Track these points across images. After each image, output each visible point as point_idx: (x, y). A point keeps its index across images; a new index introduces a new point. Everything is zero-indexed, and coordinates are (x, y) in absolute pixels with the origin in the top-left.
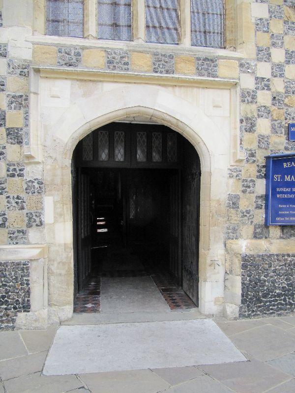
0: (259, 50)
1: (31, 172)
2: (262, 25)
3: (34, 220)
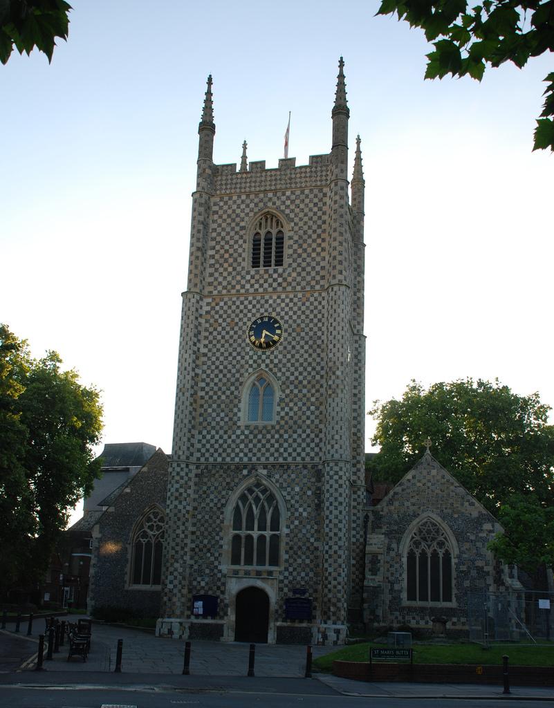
0: (285, 568)
1: (226, 601)
2: (287, 561)
3: (226, 614)
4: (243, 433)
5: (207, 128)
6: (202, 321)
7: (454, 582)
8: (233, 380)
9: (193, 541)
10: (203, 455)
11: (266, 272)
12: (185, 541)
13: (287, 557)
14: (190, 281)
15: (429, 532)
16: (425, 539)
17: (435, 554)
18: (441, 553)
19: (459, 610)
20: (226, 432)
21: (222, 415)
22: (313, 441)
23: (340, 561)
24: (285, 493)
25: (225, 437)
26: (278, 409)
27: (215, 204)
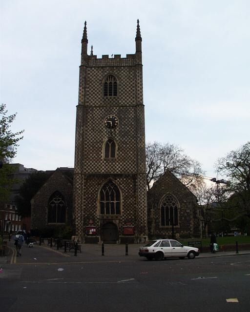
2: (123, 212)
4: (103, 162)
5: (85, 41)
7: (179, 218)
8: (98, 141)
9: (84, 206)
10: (87, 171)
11: (111, 98)
13: (123, 211)
14: (79, 101)
15: (169, 200)
17: (171, 208)
18: (174, 207)
20: (96, 162)
21: (94, 155)
22: (132, 165)
23: (145, 212)
24: (121, 186)
25: (96, 164)
26: (118, 153)
27: (89, 70)
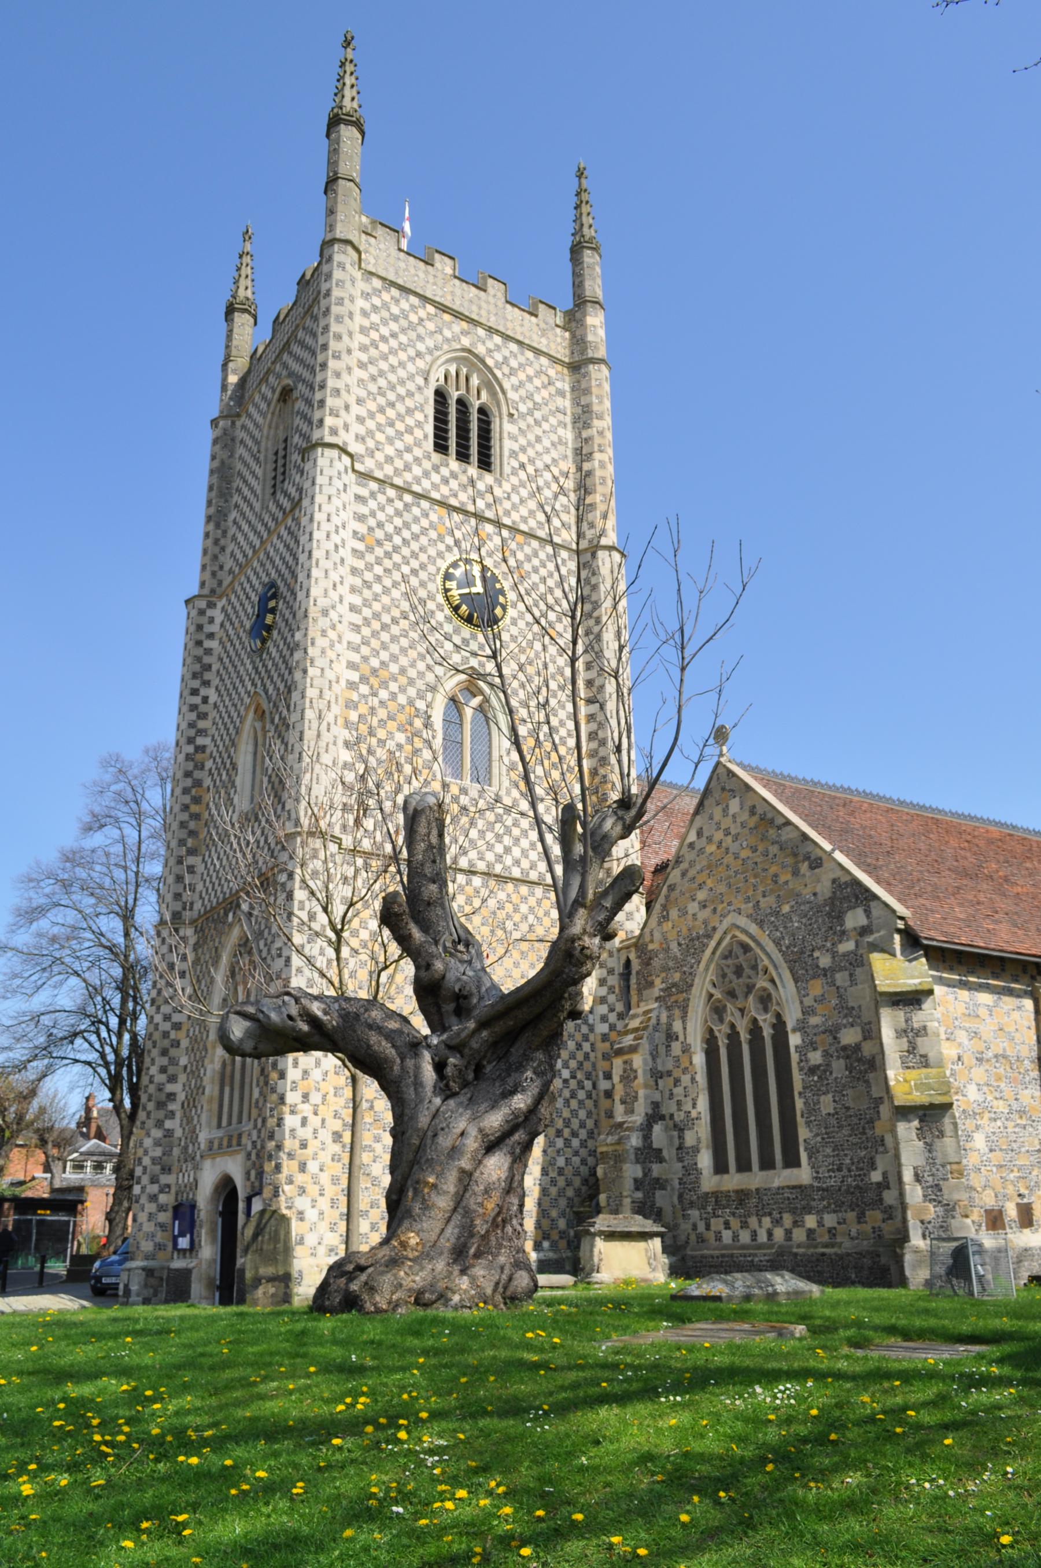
6: (214, 644)
7: (799, 1104)
12: (170, 1088)
16: (732, 994)
17: (755, 1030)
18: (766, 1022)
19: (819, 1189)
